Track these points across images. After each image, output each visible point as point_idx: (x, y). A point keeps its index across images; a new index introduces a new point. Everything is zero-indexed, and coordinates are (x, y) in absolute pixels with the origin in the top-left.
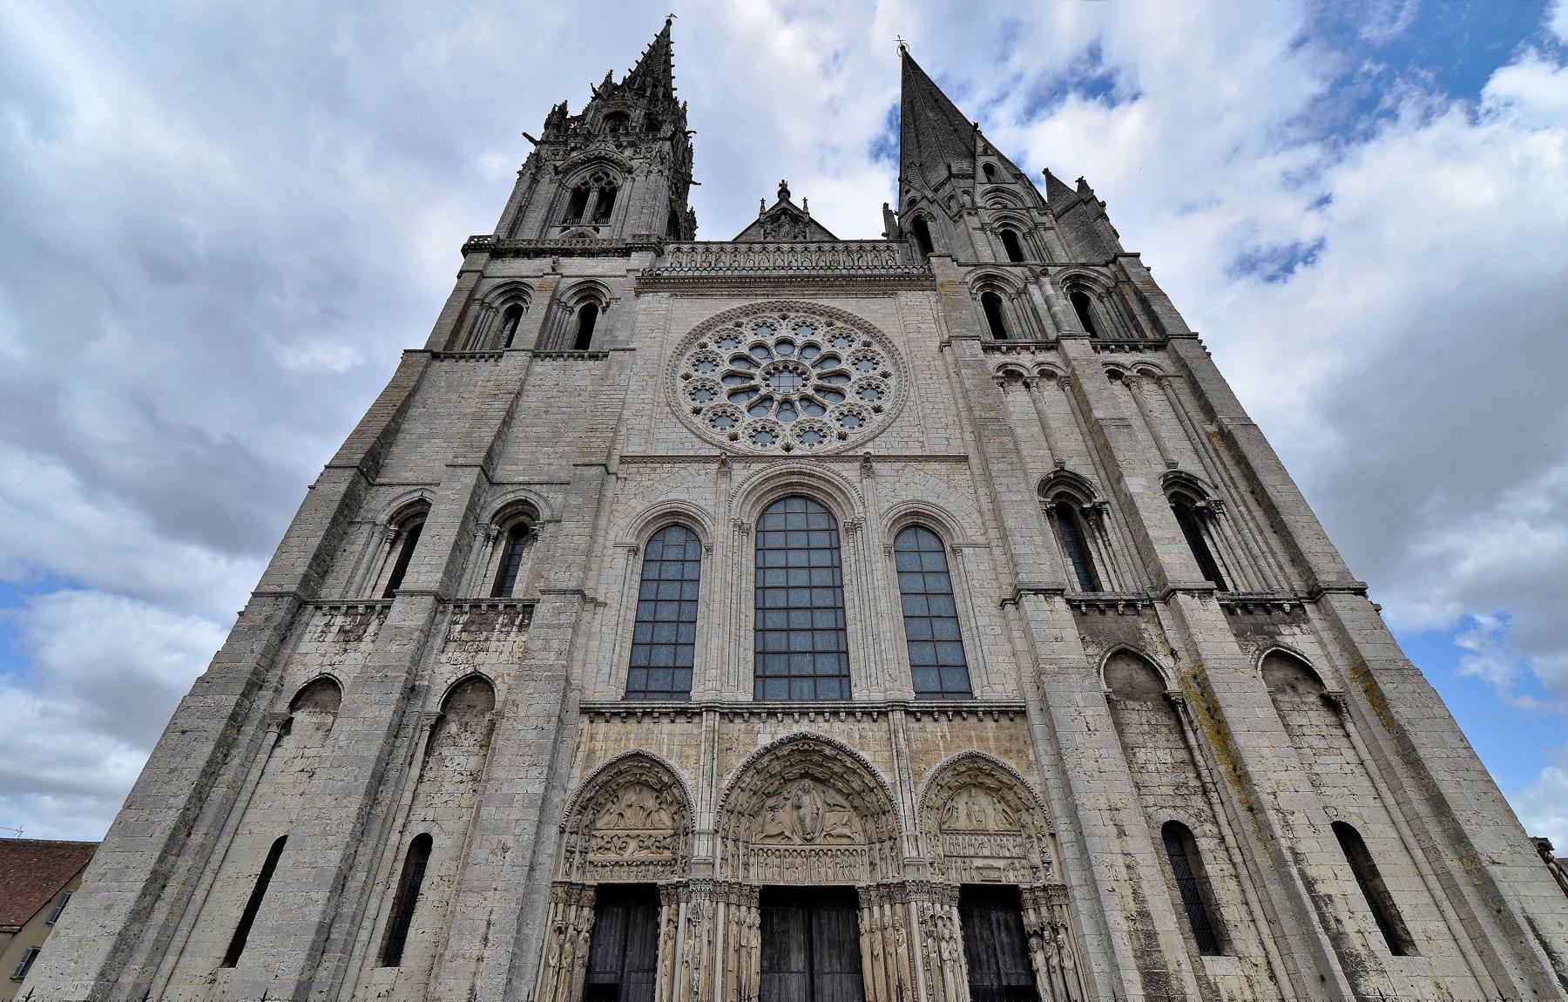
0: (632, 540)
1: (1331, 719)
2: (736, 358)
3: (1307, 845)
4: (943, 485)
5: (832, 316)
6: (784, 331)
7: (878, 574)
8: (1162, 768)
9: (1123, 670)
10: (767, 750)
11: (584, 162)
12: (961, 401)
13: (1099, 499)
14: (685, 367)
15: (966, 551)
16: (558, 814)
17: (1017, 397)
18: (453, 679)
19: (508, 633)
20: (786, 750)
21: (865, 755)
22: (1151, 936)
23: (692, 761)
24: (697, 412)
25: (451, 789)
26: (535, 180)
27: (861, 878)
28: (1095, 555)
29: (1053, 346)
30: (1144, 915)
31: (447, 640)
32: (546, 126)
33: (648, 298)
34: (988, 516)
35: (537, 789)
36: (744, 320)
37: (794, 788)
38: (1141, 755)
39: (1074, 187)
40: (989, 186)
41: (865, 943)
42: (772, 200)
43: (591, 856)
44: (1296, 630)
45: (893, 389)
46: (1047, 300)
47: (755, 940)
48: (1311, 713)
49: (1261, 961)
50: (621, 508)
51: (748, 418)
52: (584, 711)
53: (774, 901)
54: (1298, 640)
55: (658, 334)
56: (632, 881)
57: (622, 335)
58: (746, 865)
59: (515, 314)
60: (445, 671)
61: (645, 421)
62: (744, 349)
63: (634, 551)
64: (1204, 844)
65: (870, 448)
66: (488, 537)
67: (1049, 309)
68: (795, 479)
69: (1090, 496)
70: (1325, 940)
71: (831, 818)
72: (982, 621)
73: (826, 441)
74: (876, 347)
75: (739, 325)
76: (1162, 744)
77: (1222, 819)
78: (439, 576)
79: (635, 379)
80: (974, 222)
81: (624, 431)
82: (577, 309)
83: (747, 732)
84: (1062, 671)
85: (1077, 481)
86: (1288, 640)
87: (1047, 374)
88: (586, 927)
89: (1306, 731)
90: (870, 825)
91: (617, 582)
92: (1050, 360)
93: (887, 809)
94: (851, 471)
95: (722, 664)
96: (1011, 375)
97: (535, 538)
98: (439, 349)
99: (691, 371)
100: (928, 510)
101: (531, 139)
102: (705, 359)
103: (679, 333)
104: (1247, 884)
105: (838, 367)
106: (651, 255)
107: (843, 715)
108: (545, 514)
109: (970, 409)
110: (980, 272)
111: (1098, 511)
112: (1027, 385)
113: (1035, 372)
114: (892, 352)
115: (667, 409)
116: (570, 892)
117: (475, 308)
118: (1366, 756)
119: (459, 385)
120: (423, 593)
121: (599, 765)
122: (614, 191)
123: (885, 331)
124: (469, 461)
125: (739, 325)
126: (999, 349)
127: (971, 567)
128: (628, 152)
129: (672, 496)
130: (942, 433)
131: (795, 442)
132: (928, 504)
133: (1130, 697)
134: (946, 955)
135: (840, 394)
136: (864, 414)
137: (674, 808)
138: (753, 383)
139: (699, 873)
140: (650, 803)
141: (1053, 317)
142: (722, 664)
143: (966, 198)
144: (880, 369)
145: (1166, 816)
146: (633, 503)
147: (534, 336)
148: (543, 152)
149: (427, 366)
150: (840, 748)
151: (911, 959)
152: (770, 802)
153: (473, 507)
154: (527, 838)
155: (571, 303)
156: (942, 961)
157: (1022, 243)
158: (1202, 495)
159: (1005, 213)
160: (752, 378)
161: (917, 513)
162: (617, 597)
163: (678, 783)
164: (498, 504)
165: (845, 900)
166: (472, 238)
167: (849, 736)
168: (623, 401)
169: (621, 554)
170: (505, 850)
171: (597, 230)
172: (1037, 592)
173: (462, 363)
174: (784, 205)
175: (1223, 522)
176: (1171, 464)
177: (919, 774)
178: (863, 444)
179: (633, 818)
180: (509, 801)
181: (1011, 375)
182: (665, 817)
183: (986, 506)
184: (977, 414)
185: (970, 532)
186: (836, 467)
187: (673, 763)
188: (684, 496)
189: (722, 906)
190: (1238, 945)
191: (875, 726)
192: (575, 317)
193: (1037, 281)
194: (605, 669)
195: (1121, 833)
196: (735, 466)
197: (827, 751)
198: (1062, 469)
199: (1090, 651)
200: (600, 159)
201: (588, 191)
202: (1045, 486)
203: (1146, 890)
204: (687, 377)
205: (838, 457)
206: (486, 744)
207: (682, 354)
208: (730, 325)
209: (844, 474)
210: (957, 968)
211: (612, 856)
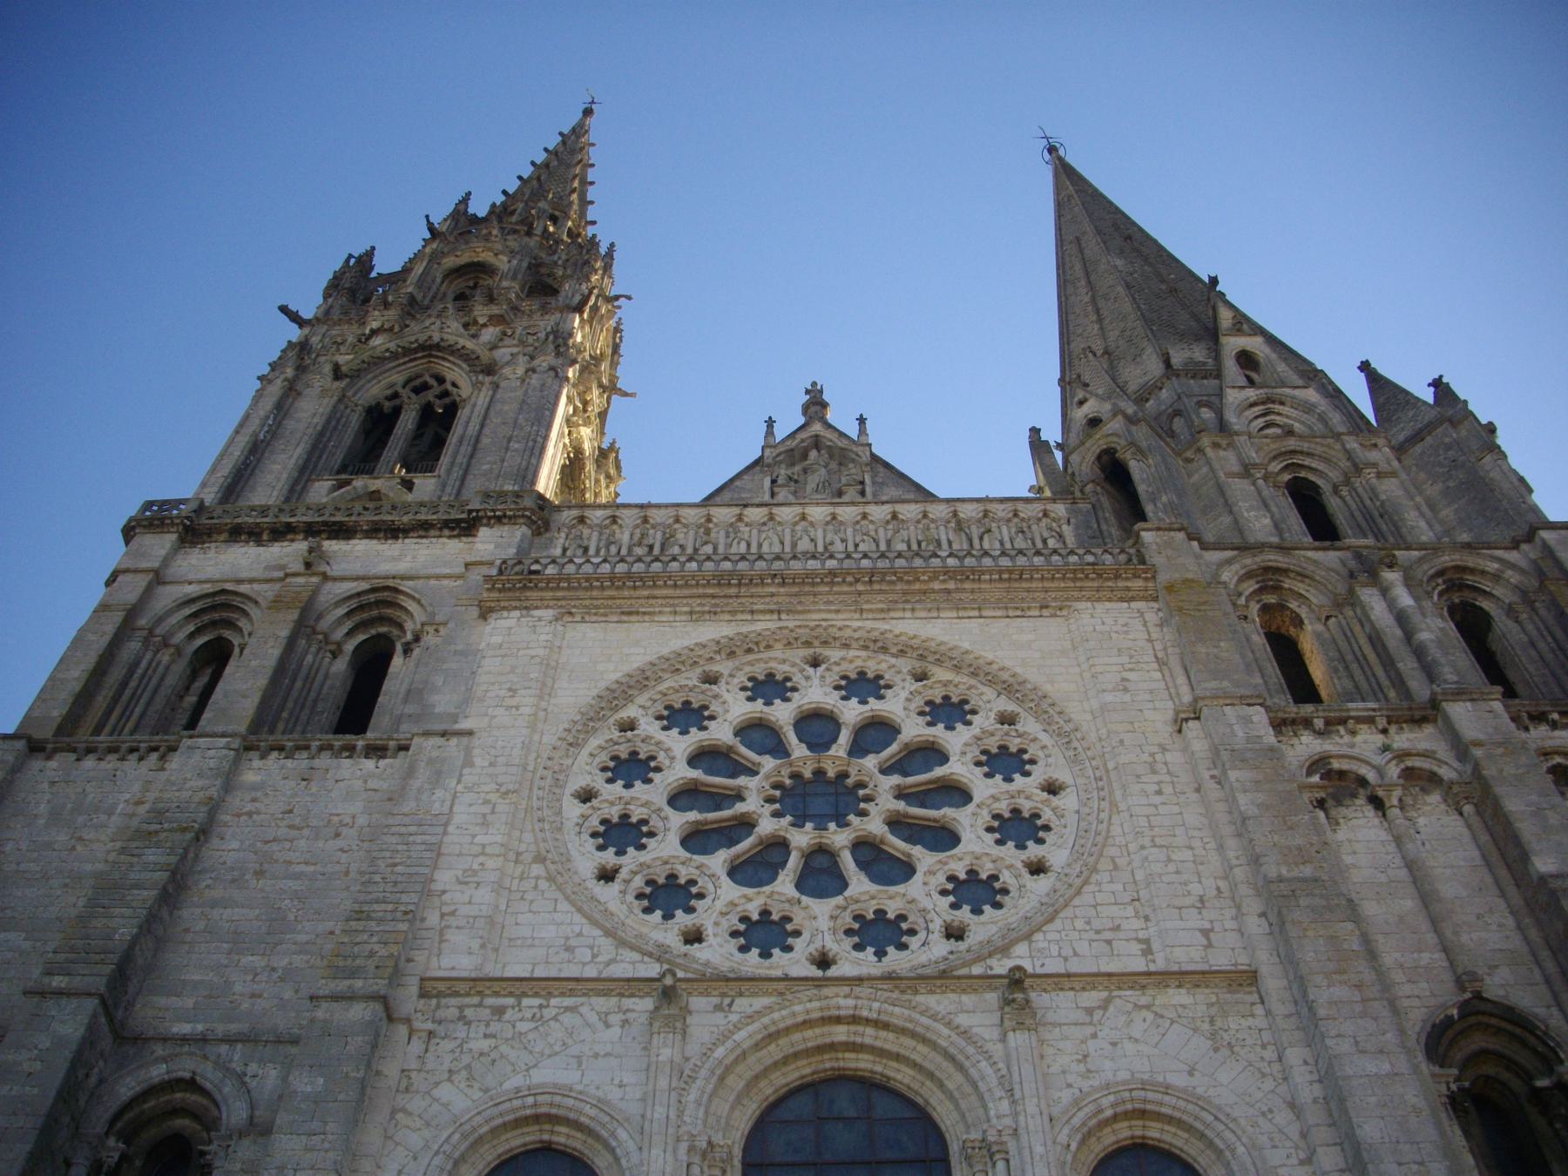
2: (703, 757)
5: (924, 661)
6: (816, 692)
11: (395, 356)
12: (1232, 843)
14: (585, 770)
17: (1360, 835)
24: (607, 875)
26: (292, 390)
29: (1426, 714)
32: (327, 295)
33: (506, 628)
34: (1315, 1116)
36: (723, 667)
39: (1428, 395)
40: (1252, 394)
42: (789, 420)
45: (1071, 819)
46: (1401, 618)
50: (416, 1104)
51: (730, 891)
55: (526, 700)
57: (442, 702)
59: (216, 657)
61: (484, 896)
62: (721, 732)
67: (1409, 635)
68: (841, 1033)
73: (915, 942)
74: (1029, 725)
75: (711, 679)
80: (1227, 460)
81: (433, 919)
82: (350, 647)
87: (1419, 779)
92: (1423, 746)
94: (976, 1014)
98: (45, 733)
99: (598, 781)
100: (1168, 1105)
101: (294, 317)
103: (573, 696)
105: (939, 772)
106: (520, 532)
108: (235, 1112)
109: (1255, 861)
110: (1250, 561)
112: (1377, 803)
113: (1394, 771)
114: (1067, 736)
115: (537, 869)
117: (133, 646)
122: (452, 410)
123: (1048, 688)
124: (77, 983)
125: (711, 679)
126: (1307, 723)
128: (489, 334)
129: (539, 1076)
130: (1194, 920)
131: (840, 947)
132: (1167, 1089)
135: (944, 838)
136: (1006, 877)
138: (740, 808)
141: (1419, 652)
143: (1206, 414)
144: (1039, 774)
146: (445, 1092)
147: (248, 707)
148: (315, 340)
155: (339, 634)
157: (1333, 504)
159: (1292, 443)
161: (1142, 1114)
164: (127, 1087)
166: (149, 505)
168: (437, 851)
171: (408, 485)
173: (89, 763)
174: (817, 427)
178: (1004, 950)
181: (1337, 786)
183: (1307, 1089)
184: (1272, 869)
186: (940, 1002)
188: (569, 1077)
192: (341, 666)
193: (1374, 578)
196: (698, 1003)
200: (431, 349)
201: (397, 411)
204: (586, 796)
205: (943, 978)
209: (963, 1020)
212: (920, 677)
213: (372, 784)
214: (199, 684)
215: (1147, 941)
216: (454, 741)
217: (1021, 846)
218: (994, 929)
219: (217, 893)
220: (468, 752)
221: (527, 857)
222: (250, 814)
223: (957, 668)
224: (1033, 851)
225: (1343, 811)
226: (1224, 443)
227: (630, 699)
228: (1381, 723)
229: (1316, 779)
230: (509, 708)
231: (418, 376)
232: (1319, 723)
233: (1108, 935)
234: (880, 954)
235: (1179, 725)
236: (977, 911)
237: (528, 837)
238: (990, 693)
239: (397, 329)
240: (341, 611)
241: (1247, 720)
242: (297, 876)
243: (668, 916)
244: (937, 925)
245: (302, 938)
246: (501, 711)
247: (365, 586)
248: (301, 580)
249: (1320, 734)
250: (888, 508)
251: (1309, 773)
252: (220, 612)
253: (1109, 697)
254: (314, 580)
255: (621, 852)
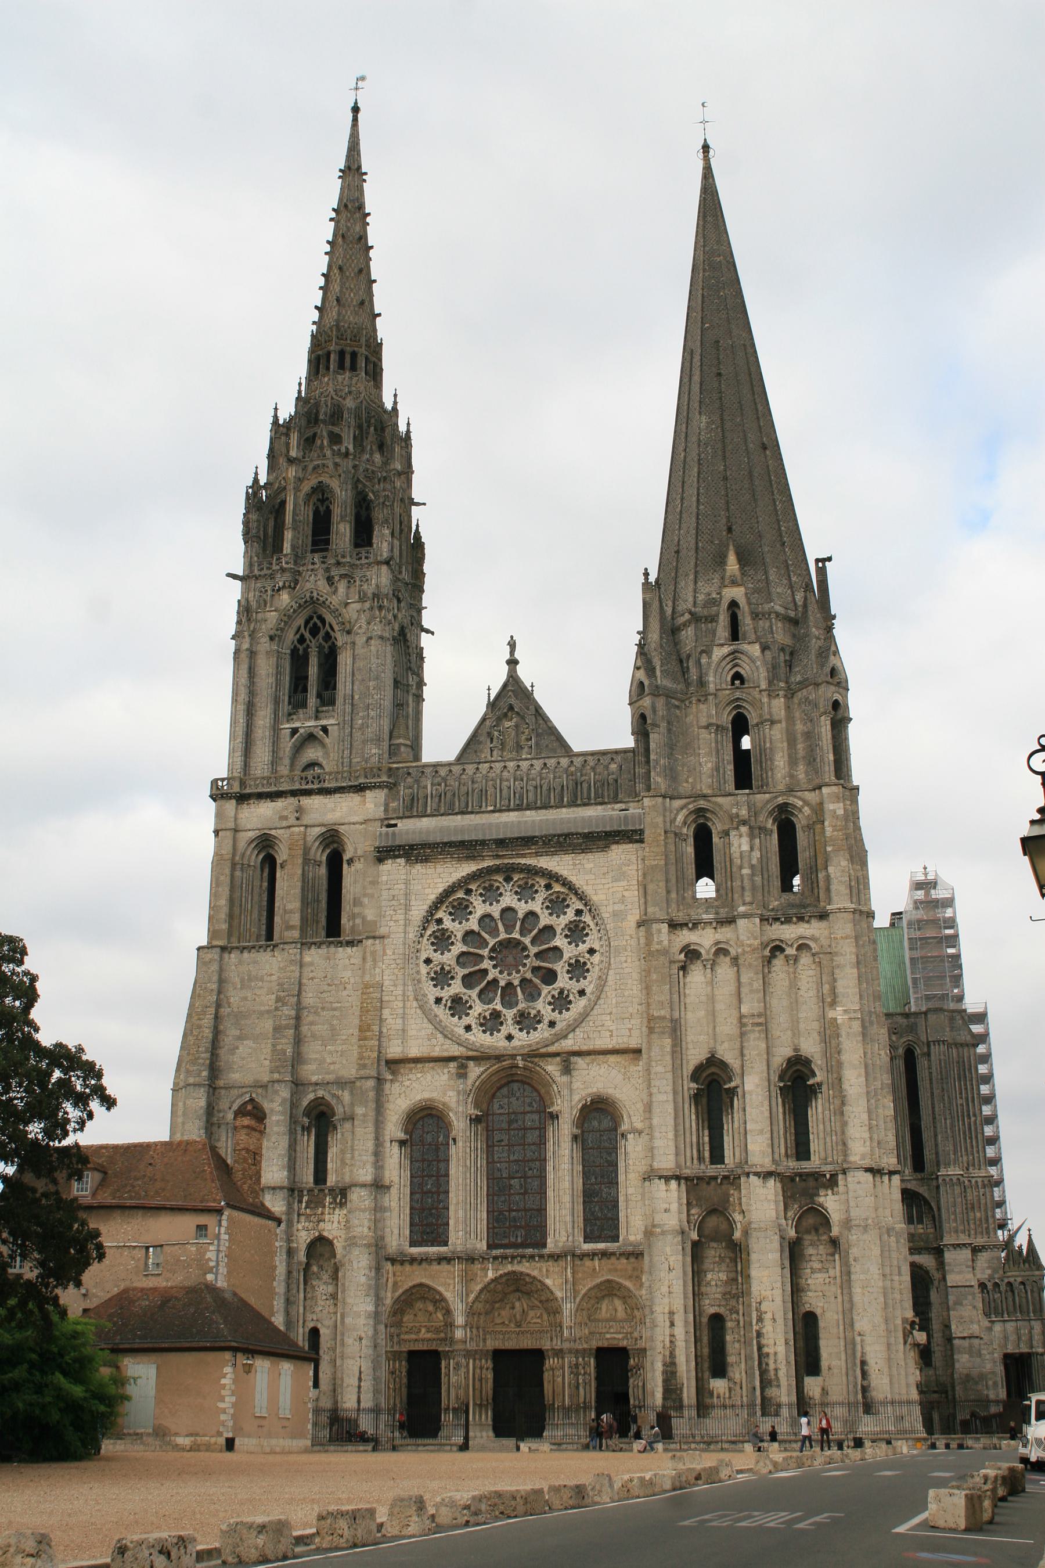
0: (402, 1136)
1: (831, 1250)
2: (469, 934)
3: (768, 1328)
4: (620, 1077)
7: (567, 1159)
8: (719, 1283)
9: (713, 1221)
10: (492, 1280)
13: (733, 1084)
14: (427, 950)
15: (630, 1136)
16: (384, 1318)
18: (309, 1240)
19: (334, 1209)
20: (504, 1279)
21: (548, 1282)
22: (674, 1373)
23: (452, 1287)
25: (323, 1303)
26: (252, 654)
27: (546, 1345)
28: (725, 1127)
30: (673, 1364)
31: (299, 1215)
33: (389, 866)
35: (371, 1308)
36: (473, 887)
37: (512, 1296)
38: (709, 1276)
41: (546, 1375)
42: (499, 677)
43: (402, 1336)
44: (830, 1192)
45: (597, 968)
47: (490, 1375)
48: (821, 1247)
49: (738, 1381)
52: (387, 1259)
53: (498, 1355)
54: (830, 1202)
56: (425, 1348)
57: (370, 915)
58: (484, 1340)
60: (303, 1237)
62: (473, 924)
63: (402, 1143)
64: (729, 1324)
65: (568, 1044)
66: (303, 1128)
69: (730, 1080)
70: (757, 1373)
71: (531, 1313)
72: (630, 1191)
76: (723, 1269)
77: (741, 1313)
78: (286, 1173)
79: (386, 972)
82: (324, 858)
83: (483, 1269)
84: (663, 1233)
85: (723, 1065)
86: (821, 1199)
88: (404, 1370)
89: (813, 1258)
90: (552, 1318)
91: (396, 1167)
93: (556, 1311)
94: (552, 1068)
95: (466, 1222)
96: (692, 954)
97: (335, 1128)
102: (442, 940)
103: (419, 910)
104: (743, 1346)
107: (537, 1259)
108: (339, 1110)
111: (732, 1092)
116: (394, 1356)
117: (238, 873)
118: (838, 1274)
119: (250, 980)
120: (281, 1188)
121: (401, 1291)
125: (469, 892)
126: (686, 925)
127: (629, 1149)
131: (514, 1031)
133: (713, 1239)
134: (581, 1381)
137: (444, 1311)
139: (461, 1347)
140: (431, 1308)
142: (466, 1222)
145: (712, 1310)
147: (296, 919)
149: (221, 958)
150: (534, 1278)
151: (564, 1383)
152: (497, 1305)
153: (294, 1105)
154: (370, 1333)
156: (578, 1383)
158: (814, 1074)
159: (738, 694)
160: (481, 957)
162: (396, 1179)
163: (443, 1299)
165: (538, 1355)
167: (540, 1270)
169: (396, 1145)
170: (361, 1339)
171: (325, 729)
172: (660, 1178)
175: (820, 1101)
176: (796, 1050)
177: (576, 1292)
178: (565, 1037)
179: (421, 1317)
180: (358, 1315)
182: (440, 1315)
185: (634, 1119)
187: (441, 1289)
189: (471, 1361)
190: (731, 1374)
191: (555, 1264)
194: (396, 1231)
195: (672, 1324)
196: (471, 1064)
197: (527, 1279)
198: (713, 1056)
199: (693, 1211)
200: (313, 601)
201: (306, 650)
202: (699, 1070)
203: (677, 1352)
204: (428, 961)
206: (335, 1277)
207: (422, 936)
208: (461, 894)
210: (587, 1387)
211: (413, 1336)
212: (548, 887)
213: (353, 961)
214: (266, 874)
215: (611, 1031)
216: (377, 941)
217: (578, 981)
218: (565, 1023)
219: (311, 1018)
220: (384, 946)
221: (411, 998)
222: (312, 979)
223: (564, 885)
224: (583, 984)
225: (693, 967)
226: (703, 699)
227: (437, 908)
228: (714, 924)
229: (683, 955)
230: (395, 921)
231: (311, 618)
232: (690, 925)
233: (600, 1028)
234: (528, 1033)
235: (639, 925)
236: (560, 1013)
237: (410, 988)
238: (574, 899)
239: (292, 585)
240: (317, 843)
241: (659, 931)
242: (335, 1009)
243: (460, 1018)
244: (546, 1022)
245: (344, 1037)
246: (392, 923)
247: (324, 829)
248: (296, 829)
249: (691, 929)
250: (542, 761)
251: (681, 952)
252: (265, 843)
253: (617, 907)
254: (302, 829)
255: (442, 989)
